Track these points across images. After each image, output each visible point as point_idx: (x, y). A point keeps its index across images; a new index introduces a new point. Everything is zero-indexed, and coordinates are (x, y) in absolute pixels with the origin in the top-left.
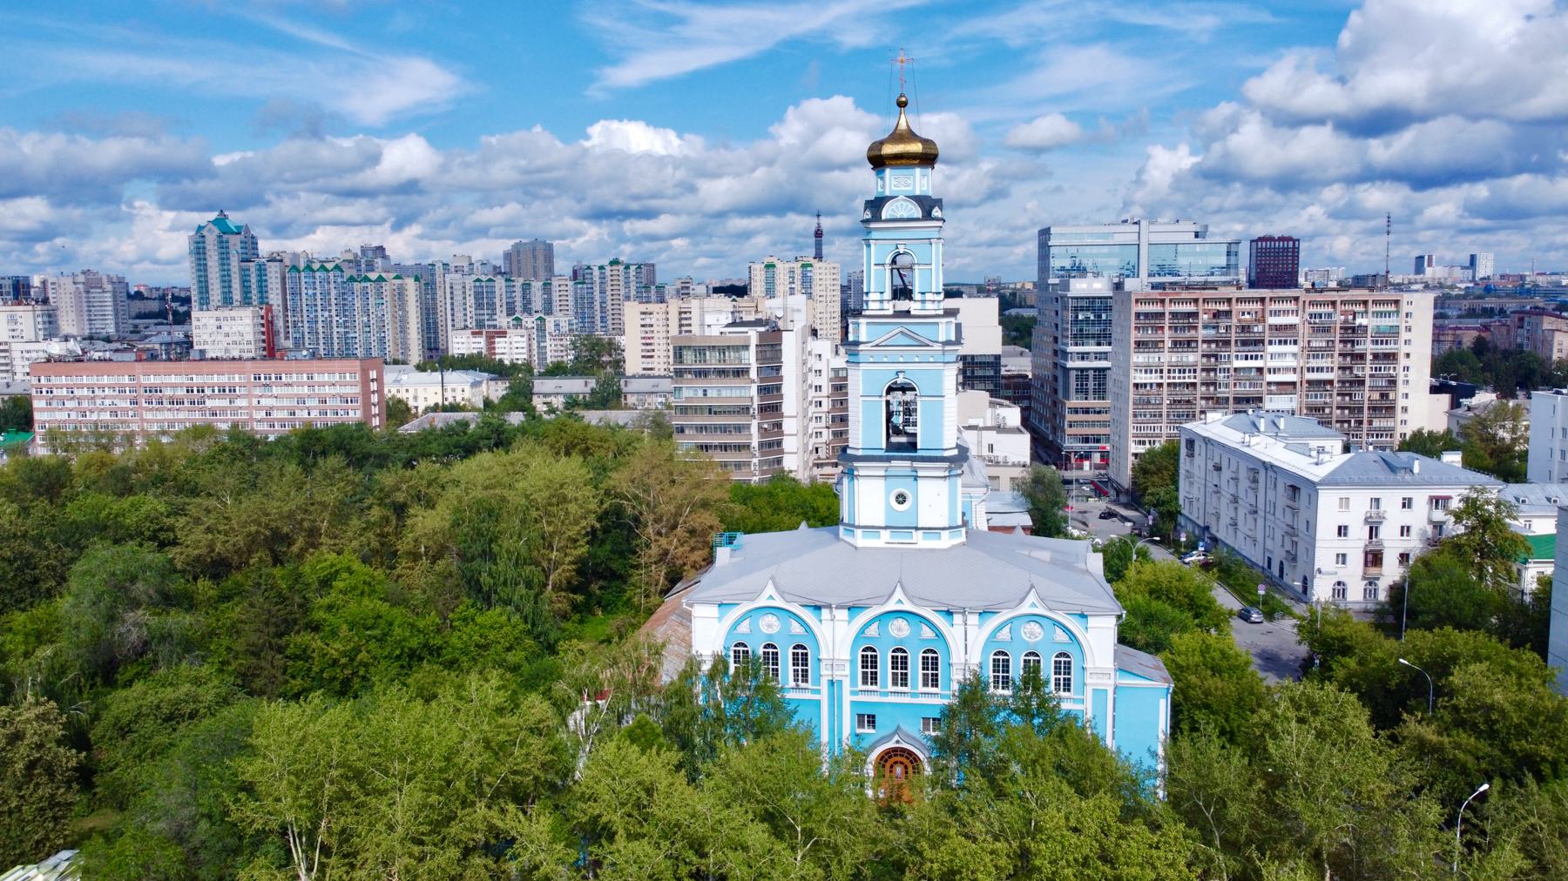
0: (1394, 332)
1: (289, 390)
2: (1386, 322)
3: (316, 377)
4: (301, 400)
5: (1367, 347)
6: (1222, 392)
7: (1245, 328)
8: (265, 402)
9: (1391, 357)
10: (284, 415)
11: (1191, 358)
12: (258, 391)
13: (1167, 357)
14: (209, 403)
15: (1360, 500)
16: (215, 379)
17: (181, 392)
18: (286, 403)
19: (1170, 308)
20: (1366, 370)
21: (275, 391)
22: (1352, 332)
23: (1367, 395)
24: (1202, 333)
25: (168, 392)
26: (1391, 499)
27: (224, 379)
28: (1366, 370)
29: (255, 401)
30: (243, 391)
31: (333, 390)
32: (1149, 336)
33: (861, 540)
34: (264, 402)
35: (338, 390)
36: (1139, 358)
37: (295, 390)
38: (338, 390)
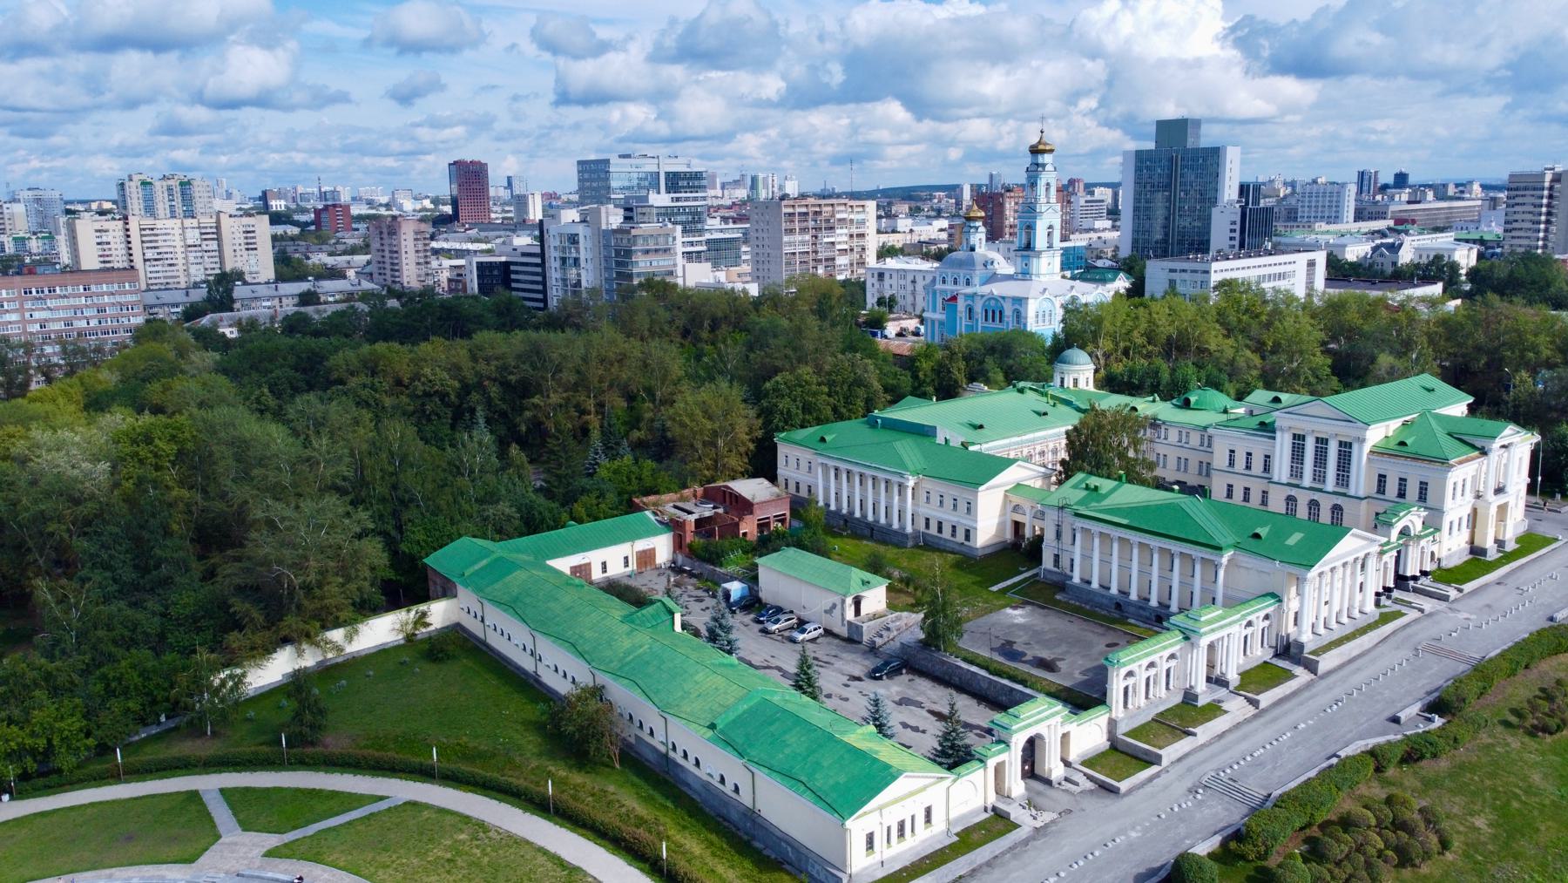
0: (863, 222)
1: (65, 302)
2: (861, 217)
3: (93, 288)
6: (820, 256)
7: (828, 221)
9: (861, 236)
10: (59, 326)
11: (807, 237)
13: (798, 238)
18: (62, 314)
19: (798, 210)
24: (811, 224)
29: (27, 315)
30: (12, 306)
31: (112, 300)
32: (789, 226)
33: (1042, 278)
34: (37, 315)
35: (118, 299)
36: (786, 239)
37: (72, 301)
38: (118, 299)
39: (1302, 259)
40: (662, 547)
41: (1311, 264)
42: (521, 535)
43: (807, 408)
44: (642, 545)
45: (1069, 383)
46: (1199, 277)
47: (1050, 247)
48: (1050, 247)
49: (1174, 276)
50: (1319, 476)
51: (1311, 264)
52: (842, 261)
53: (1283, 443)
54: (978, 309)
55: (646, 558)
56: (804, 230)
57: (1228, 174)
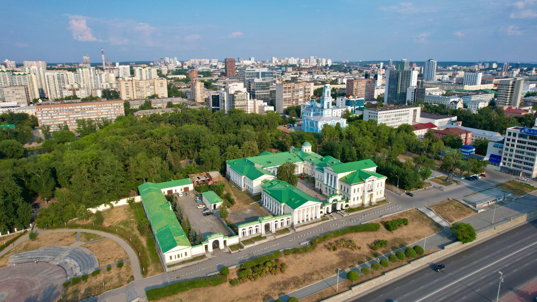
4: (110, 110)
5: (307, 91)
8: (101, 111)
9: (309, 92)
12: (99, 108)
13: (287, 94)
14: (87, 112)
15: (336, 110)
16: (88, 106)
17: (79, 110)
20: (307, 94)
21: (104, 108)
22: (305, 88)
23: (307, 98)
25: (76, 110)
26: (338, 110)
27: (90, 106)
28: (307, 94)
39: (411, 110)
40: (191, 187)
41: (415, 111)
42: (163, 182)
43: (235, 154)
44: (185, 186)
45: (304, 151)
46: (375, 115)
47: (328, 108)
48: (328, 108)
49: (370, 114)
50: (331, 184)
51: (415, 111)
52: (301, 100)
53: (326, 174)
54: (309, 123)
55: (186, 189)
56: (289, 92)
57: (413, 78)
